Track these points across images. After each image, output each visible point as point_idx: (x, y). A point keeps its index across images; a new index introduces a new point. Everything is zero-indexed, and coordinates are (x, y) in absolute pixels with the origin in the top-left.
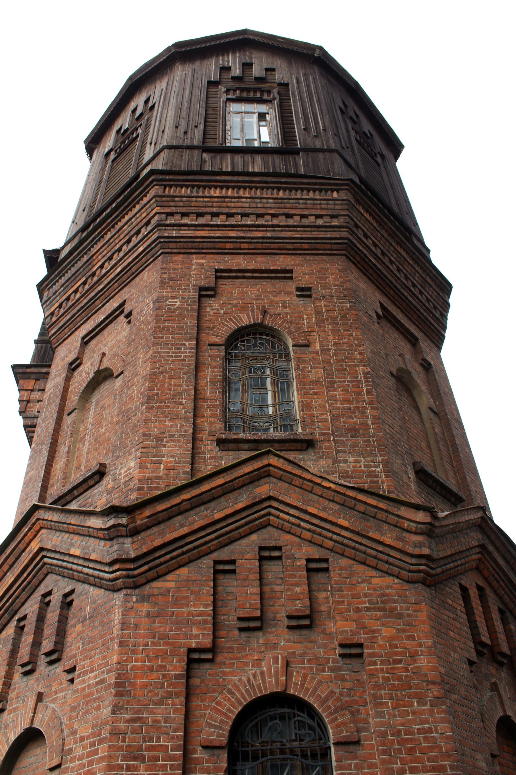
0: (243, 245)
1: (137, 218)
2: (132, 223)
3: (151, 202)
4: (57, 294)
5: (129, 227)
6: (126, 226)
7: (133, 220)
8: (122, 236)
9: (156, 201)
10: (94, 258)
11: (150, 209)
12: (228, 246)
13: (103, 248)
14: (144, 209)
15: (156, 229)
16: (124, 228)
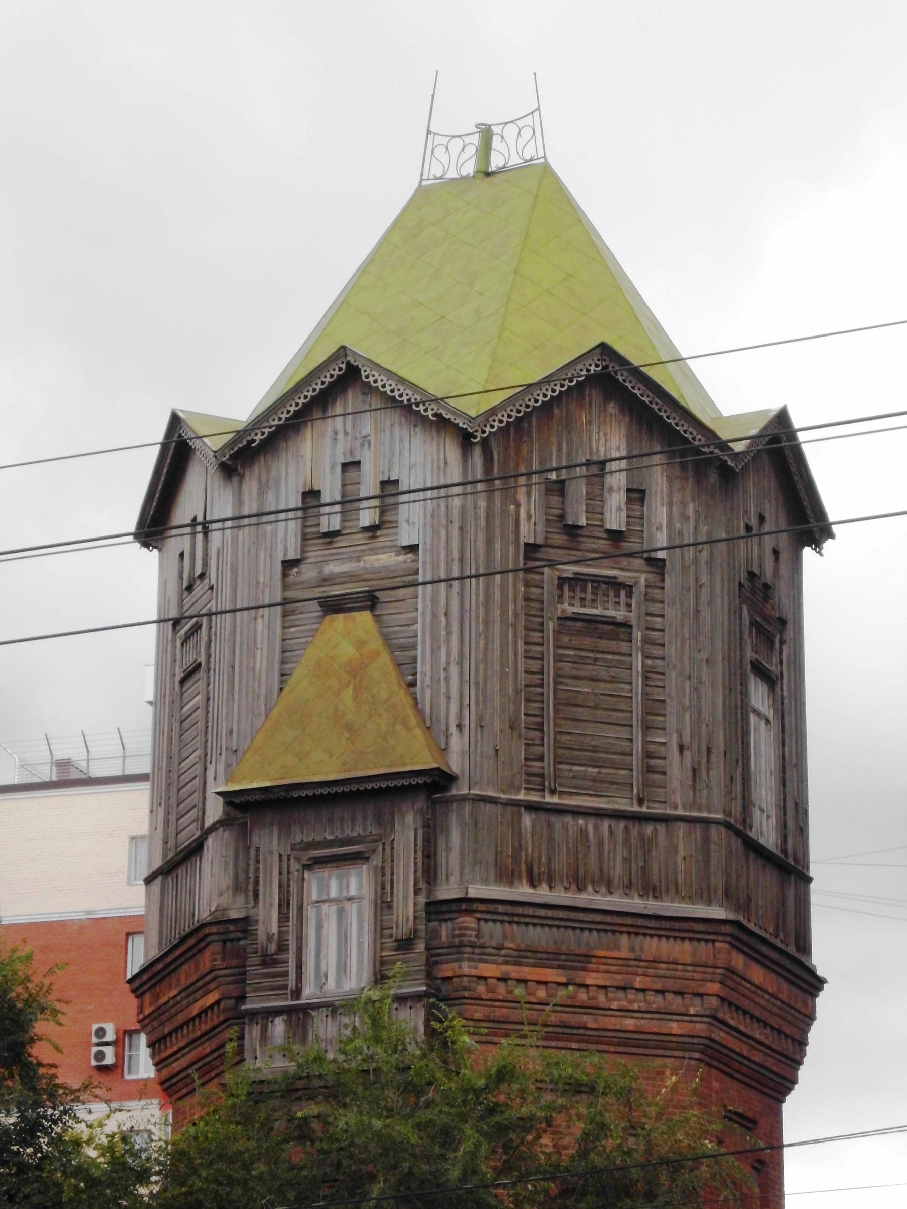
0: (744, 1070)
1: (686, 971)
2: (676, 970)
3: (718, 971)
4: (503, 952)
5: (668, 969)
6: (665, 966)
7: (680, 967)
8: (651, 971)
9: (722, 975)
10: (594, 960)
11: (709, 976)
12: (737, 1066)
13: (614, 961)
14: (703, 969)
15: (705, 1019)
16: (661, 965)
